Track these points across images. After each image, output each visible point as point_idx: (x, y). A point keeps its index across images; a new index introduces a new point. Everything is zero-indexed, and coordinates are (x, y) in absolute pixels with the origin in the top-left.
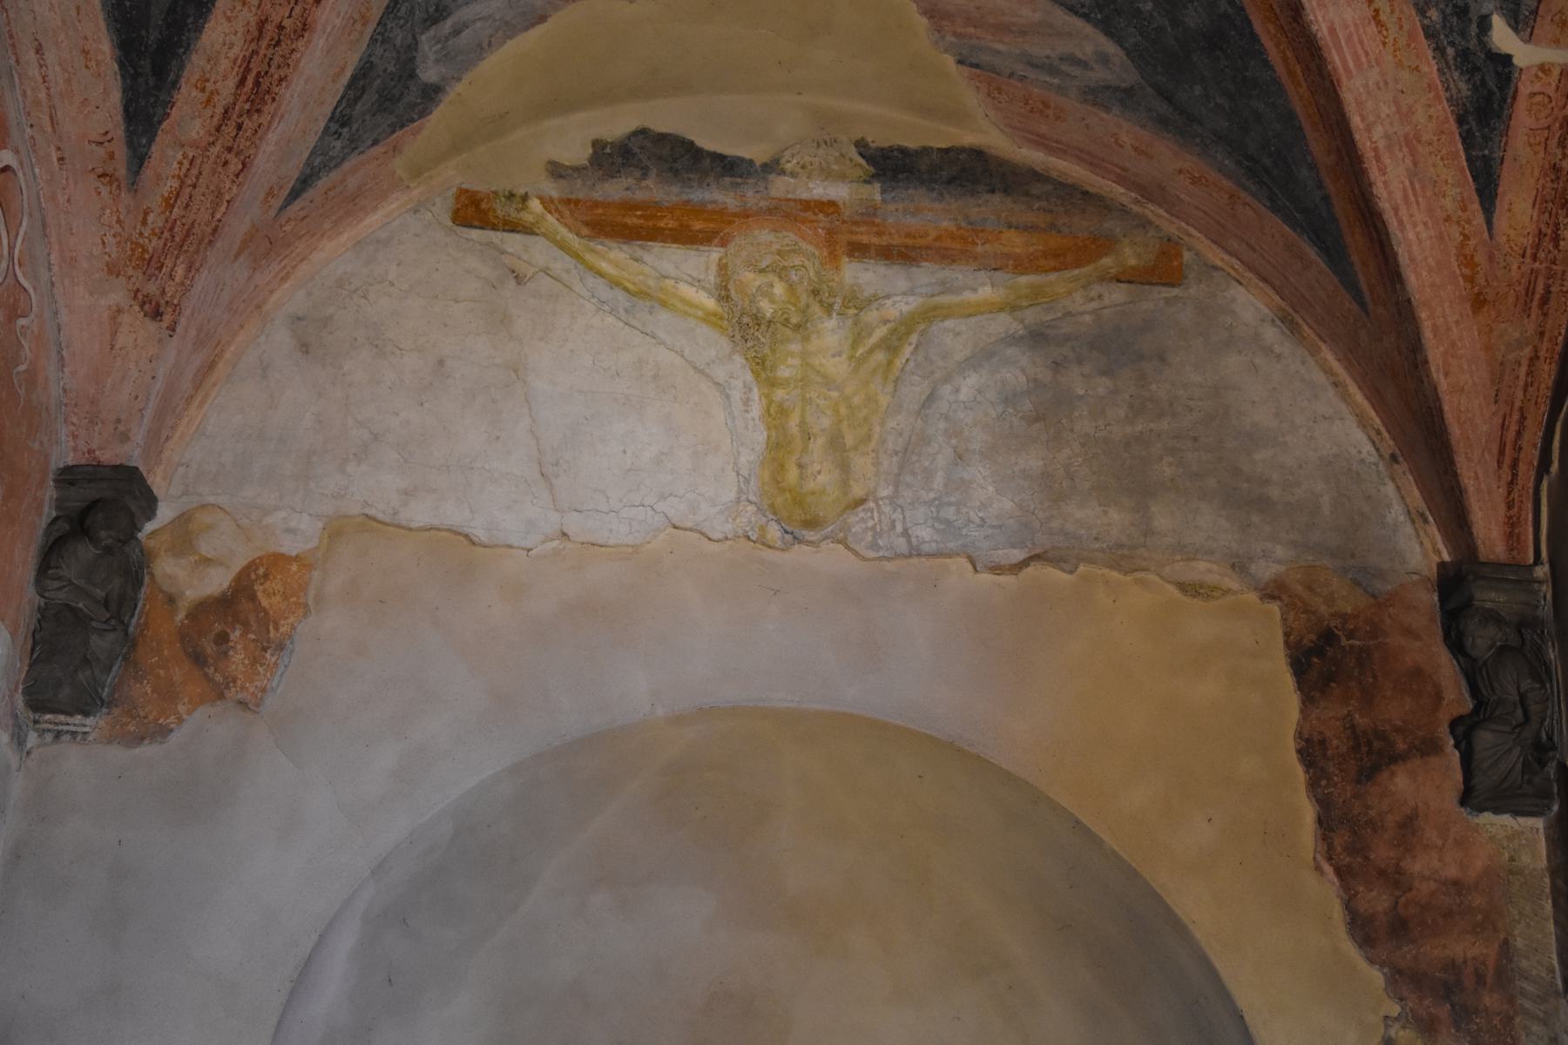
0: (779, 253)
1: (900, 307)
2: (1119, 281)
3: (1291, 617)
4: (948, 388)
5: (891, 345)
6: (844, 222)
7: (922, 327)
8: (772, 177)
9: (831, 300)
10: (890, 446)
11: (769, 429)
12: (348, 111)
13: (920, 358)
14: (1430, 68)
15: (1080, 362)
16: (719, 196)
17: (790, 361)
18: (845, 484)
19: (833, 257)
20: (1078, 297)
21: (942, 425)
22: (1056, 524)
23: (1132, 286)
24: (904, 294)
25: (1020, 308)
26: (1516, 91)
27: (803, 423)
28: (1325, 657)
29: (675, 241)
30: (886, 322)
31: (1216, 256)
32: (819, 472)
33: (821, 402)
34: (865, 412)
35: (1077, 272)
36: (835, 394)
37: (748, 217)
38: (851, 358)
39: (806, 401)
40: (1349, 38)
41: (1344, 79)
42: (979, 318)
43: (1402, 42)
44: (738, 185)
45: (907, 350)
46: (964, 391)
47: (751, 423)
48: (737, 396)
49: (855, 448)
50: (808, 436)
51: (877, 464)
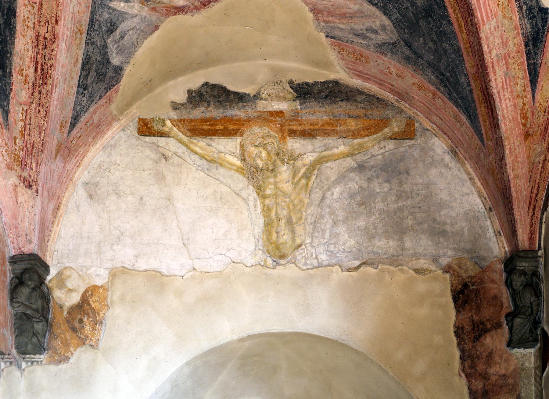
0: (263, 137)
1: (309, 158)
2: (391, 139)
3: (453, 279)
4: (329, 193)
5: (307, 176)
6: (287, 120)
7: (318, 166)
8: (258, 101)
9: (284, 157)
10: (309, 220)
11: (264, 217)
12: (84, 82)
13: (318, 181)
15: (378, 178)
16: (237, 112)
17: (270, 186)
18: (293, 239)
19: (283, 137)
20: (376, 148)
21: (328, 210)
23: (396, 141)
24: (311, 152)
25: (355, 155)
27: (277, 213)
28: (465, 294)
29: (223, 135)
30: (305, 165)
31: (427, 124)
32: (284, 235)
33: (283, 204)
34: (299, 206)
35: (375, 136)
36: (288, 200)
37: (249, 121)
38: (293, 183)
39: (277, 204)
42: (340, 160)
45: (314, 177)
46: (335, 194)
47: (258, 216)
48: (251, 204)
49: (297, 223)
50: (279, 219)
51: (305, 229)
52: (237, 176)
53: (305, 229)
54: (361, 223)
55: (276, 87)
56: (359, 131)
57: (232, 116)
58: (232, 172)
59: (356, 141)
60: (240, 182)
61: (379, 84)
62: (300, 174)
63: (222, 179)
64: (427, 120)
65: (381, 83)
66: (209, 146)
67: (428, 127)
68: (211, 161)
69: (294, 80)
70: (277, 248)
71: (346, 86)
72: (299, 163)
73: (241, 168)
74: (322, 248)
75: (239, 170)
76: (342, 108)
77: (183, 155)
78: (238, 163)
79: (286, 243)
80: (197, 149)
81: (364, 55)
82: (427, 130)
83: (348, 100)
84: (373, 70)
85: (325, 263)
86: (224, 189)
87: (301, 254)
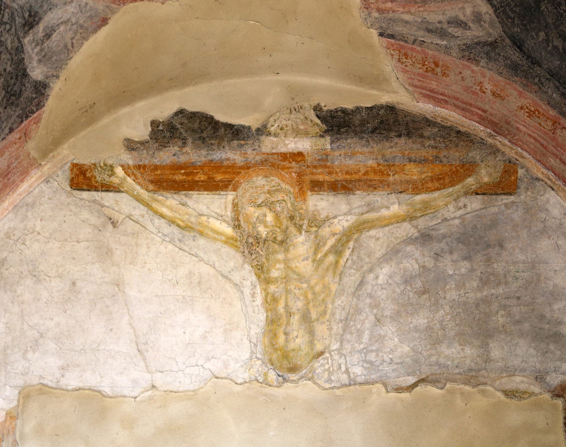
0: (269, 192)
1: (342, 223)
2: (477, 194)
4: (371, 276)
5: (337, 251)
6: (308, 167)
7: (356, 236)
8: (263, 138)
9: (301, 223)
10: (338, 316)
11: (267, 311)
13: (355, 258)
15: (451, 253)
16: (230, 154)
17: (278, 266)
18: (312, 343)
19: (302, 192)
20: (451, 207)
21: (368, 301)
22: (434, 359)
23: (485, 197)
24: (345, 214)
25: (416, 218)
27: (286, 305)
29: (206, 189)
30: (334, 234)
32: (297, 337)
33: (297, 291)
34: (323, 295)
35: (451, 189)
36: (305, 286)
37: (249, 168)
38: (314, 261)
39: (288, 292)
42: (391, 227)
44: (242, 146)
45: (348, 252)
46: (381, 277)
47: (256, 309)
49: (318, 320)
50: (290, 314)
51: (330, 329)
52: (227, 250)
53: (330, 329)
54: (421, 320)
55: (293, 116)
56: (424, 182)
57: (221, 161)
58: (219, 245)
59: (418, 198)
60: (231, 260)
61: (463, 109)
62: (327, 248)
63: (201, 254)
64: (538, 164)
65: (465, 108)
66: (183, 205)
67: (540, 176)
68: (186, 228)
69: (323, 105)
70: (286, 356)
71: (407, 114)
72: (325, 231)
73: (232, 239)
74: (356, 358)
75: (230, 241)
76: (397, 148)
77: (141, 219)
78: (229, 231)
79: (300, 349)
80: (164, 210)
81: (441, 63)
82: (538, 179)
83: (409, 135)
84: (454, 87)
85: (359, 379)
86: (205, 269)
87: (323, 365)
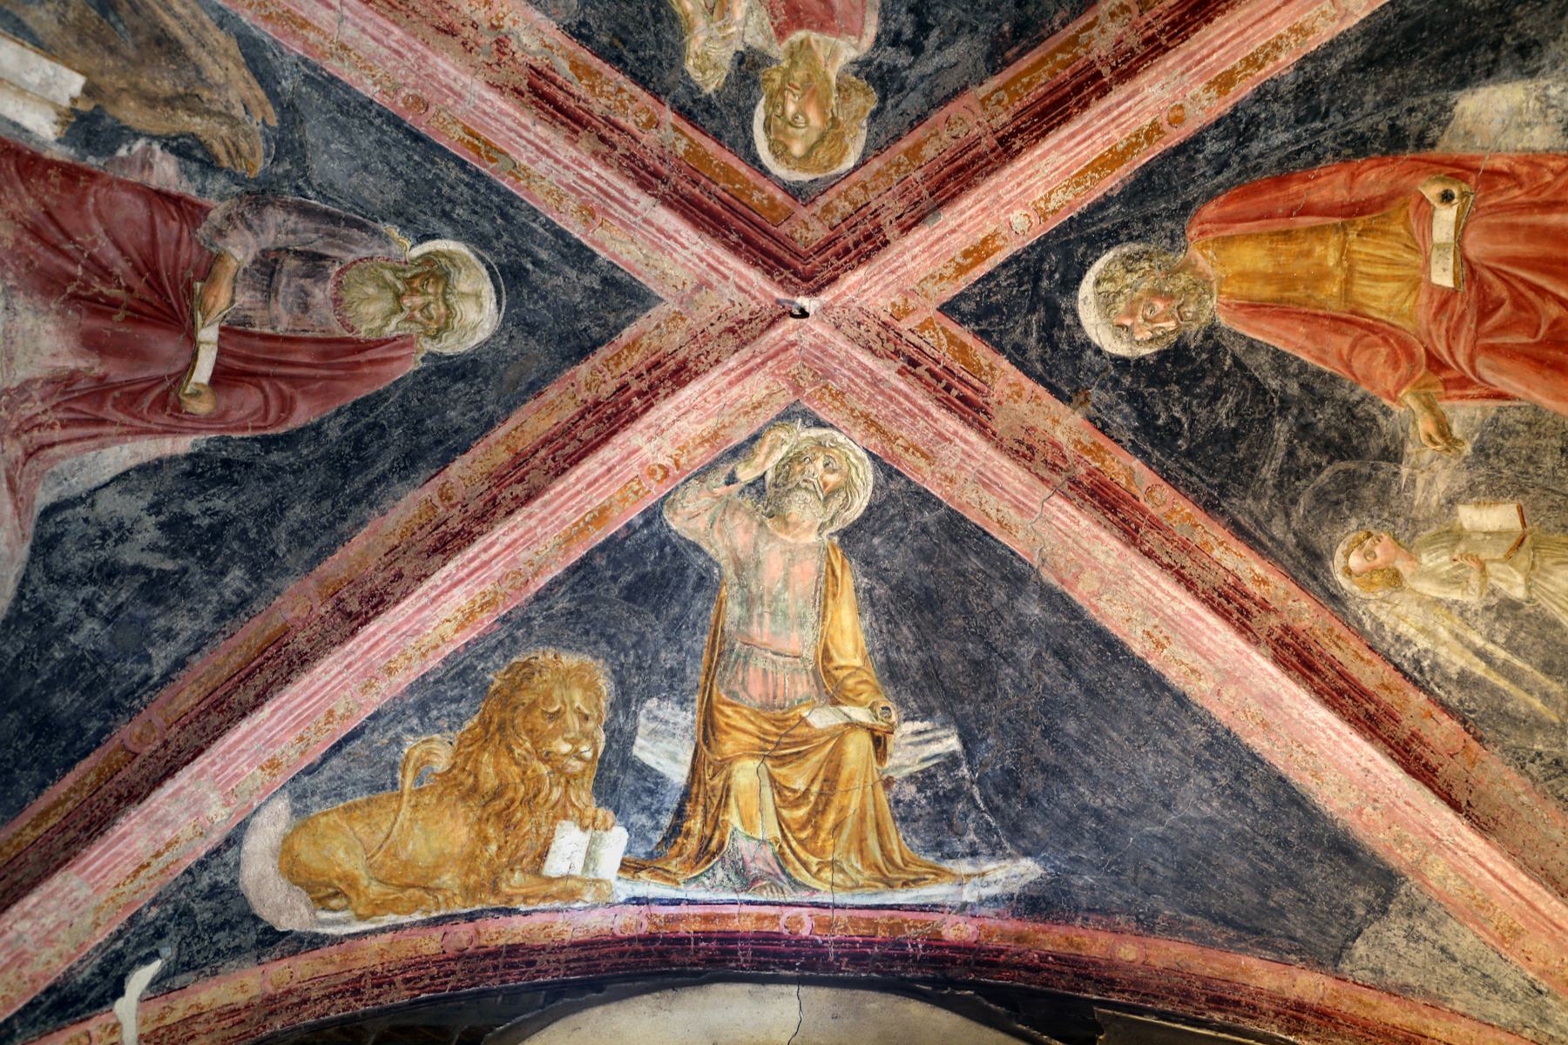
14: (101, 936)
26: (88, 1019)
40: (119, 854)
41: (75, 869)
43: (122, 900)
